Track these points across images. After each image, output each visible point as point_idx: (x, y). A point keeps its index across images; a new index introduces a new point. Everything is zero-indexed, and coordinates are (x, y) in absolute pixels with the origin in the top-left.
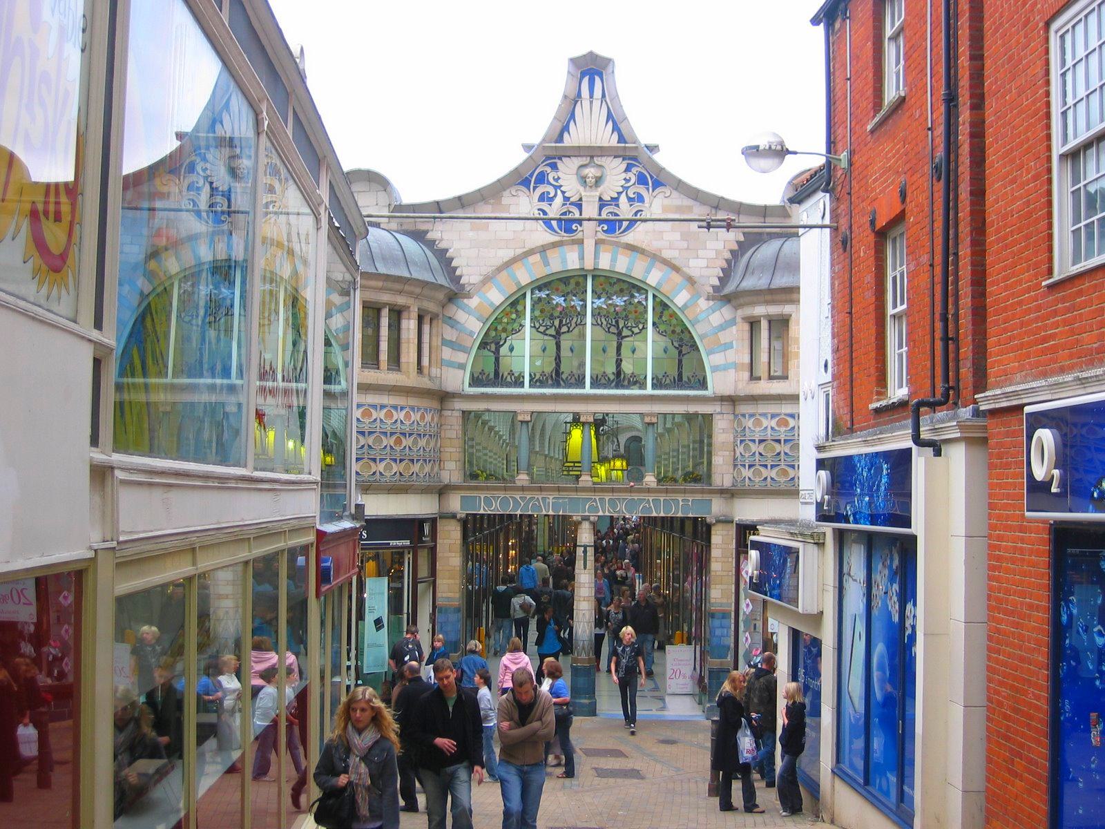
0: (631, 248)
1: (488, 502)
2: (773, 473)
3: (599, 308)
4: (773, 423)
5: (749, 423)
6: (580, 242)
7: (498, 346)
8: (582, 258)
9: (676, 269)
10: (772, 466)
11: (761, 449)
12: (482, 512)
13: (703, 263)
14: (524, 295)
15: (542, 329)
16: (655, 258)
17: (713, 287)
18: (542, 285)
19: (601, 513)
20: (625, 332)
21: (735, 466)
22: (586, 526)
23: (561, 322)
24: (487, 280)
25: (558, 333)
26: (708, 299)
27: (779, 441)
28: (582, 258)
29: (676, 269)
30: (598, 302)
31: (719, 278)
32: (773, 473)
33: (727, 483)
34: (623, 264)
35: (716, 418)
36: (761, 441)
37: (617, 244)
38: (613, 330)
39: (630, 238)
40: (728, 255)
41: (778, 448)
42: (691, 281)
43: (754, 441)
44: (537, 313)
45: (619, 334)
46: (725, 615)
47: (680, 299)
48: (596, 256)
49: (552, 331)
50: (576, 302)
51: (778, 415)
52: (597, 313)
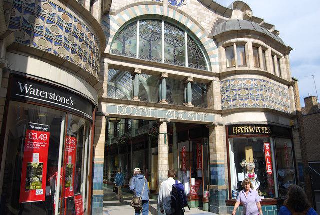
0: (181, 12)
1: (121, 110)
2: (246, 102)
3: (167, 34)
4: (244, 82)
5: (232, 83)
6: (162, 5)
7: (125, 41)
8: (163, 11)
9: (197, 24)
10: (246, 100)
11: (239, 92)
12: (117, 114)
13: (206, 25)
14: (137, 22)
15: (144, 37)
16: (190, 18)
17: (210, 34)
18: (144, 18)
19: (172, 118)
20: (177, 45)
21: (222, 102)
22: (165, 124)
23: (152, 36)
24: (123, 10)
25: (151, 40)
26: (208, 38)
27: (248, 89)
28: (163, 11)
29: (197, 24)
30: (166, 32)
31: (212, 31)
32: (246, 102)
33: (220, 109)
34: (178, 18)
35: (214, 82)
36: (239, 90)
37: (175, 9)
38: (172, 43)
39: (180, 8)
40: (214, 24)
41: (247, 92)
42: (203, 30)
43: (236, 90)
44: (142, 31)
45: (175, 45)
46: (223, 166)
47: (199, 35)
48: (168, 12)
49: (148, 39)
50: (157, 29)
51: (246, 79)
52: (166, 35)
